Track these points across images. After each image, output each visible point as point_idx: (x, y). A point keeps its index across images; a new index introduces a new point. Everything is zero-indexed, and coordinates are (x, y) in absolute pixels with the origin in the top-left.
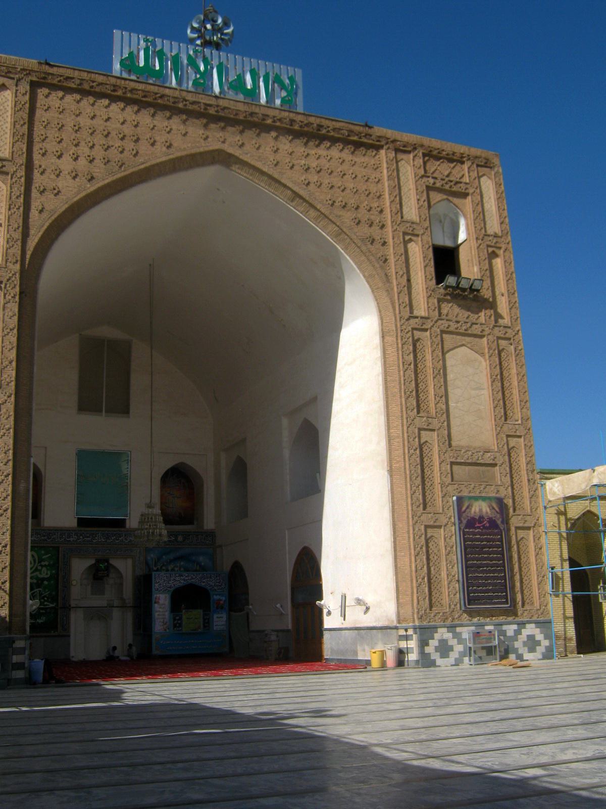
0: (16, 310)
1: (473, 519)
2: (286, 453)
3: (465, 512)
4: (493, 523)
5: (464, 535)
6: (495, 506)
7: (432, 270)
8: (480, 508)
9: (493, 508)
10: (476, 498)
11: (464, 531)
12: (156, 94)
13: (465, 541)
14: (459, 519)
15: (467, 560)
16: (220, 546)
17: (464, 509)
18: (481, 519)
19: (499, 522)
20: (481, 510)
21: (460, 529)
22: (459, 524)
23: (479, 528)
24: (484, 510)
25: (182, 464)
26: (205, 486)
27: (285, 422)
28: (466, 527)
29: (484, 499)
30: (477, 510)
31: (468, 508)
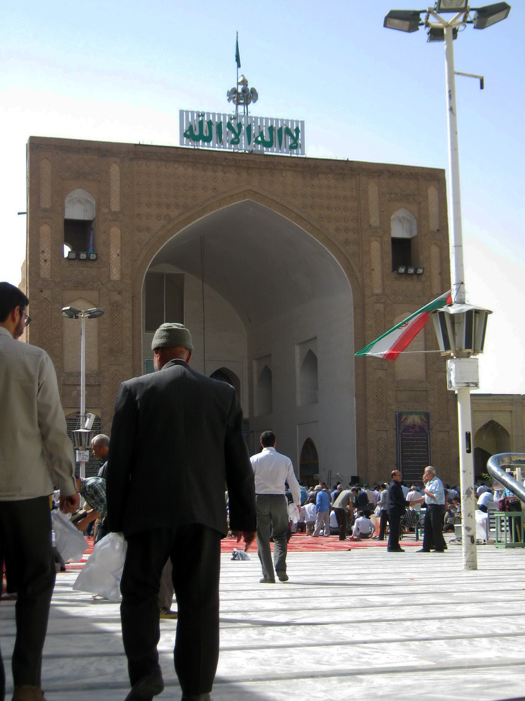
0: (130, 307)
1: (409, 426)
2: (298, 371)
3: (403, 422)
4: (421, 429)
5: (401, 436)
6: (423, 418)
7: (389, 260)
8: (414, 419)
9: (423, 420)
10: (411, 413)
11: (401, 434)
12: (208, 156)
13: (402, 440)
14: (399, 427)
15: (402, 452)
16: (253, 432)
17: (402, 420)
18: (414, 426)
19: (426, 428)
20: (414, 421)
21: (399, 432)
22: (399, 429)
23: (411, 432)
24: (416, 420)
25: (224, 368)
26: (241, 385)
27: (297, 349)
28: (403, 432)
29: (416, 413)
30: (412, 420)
31: (405, 419)
